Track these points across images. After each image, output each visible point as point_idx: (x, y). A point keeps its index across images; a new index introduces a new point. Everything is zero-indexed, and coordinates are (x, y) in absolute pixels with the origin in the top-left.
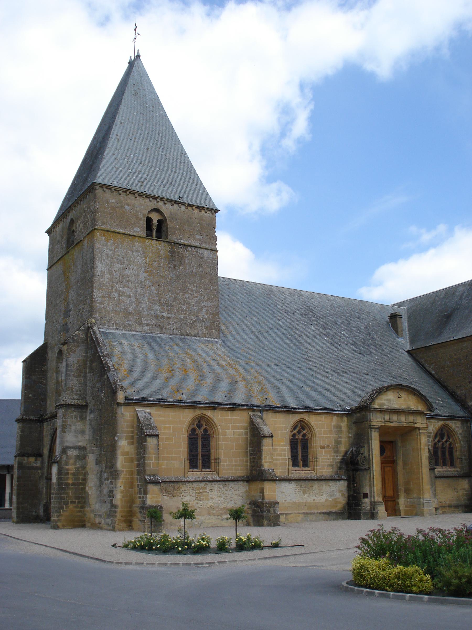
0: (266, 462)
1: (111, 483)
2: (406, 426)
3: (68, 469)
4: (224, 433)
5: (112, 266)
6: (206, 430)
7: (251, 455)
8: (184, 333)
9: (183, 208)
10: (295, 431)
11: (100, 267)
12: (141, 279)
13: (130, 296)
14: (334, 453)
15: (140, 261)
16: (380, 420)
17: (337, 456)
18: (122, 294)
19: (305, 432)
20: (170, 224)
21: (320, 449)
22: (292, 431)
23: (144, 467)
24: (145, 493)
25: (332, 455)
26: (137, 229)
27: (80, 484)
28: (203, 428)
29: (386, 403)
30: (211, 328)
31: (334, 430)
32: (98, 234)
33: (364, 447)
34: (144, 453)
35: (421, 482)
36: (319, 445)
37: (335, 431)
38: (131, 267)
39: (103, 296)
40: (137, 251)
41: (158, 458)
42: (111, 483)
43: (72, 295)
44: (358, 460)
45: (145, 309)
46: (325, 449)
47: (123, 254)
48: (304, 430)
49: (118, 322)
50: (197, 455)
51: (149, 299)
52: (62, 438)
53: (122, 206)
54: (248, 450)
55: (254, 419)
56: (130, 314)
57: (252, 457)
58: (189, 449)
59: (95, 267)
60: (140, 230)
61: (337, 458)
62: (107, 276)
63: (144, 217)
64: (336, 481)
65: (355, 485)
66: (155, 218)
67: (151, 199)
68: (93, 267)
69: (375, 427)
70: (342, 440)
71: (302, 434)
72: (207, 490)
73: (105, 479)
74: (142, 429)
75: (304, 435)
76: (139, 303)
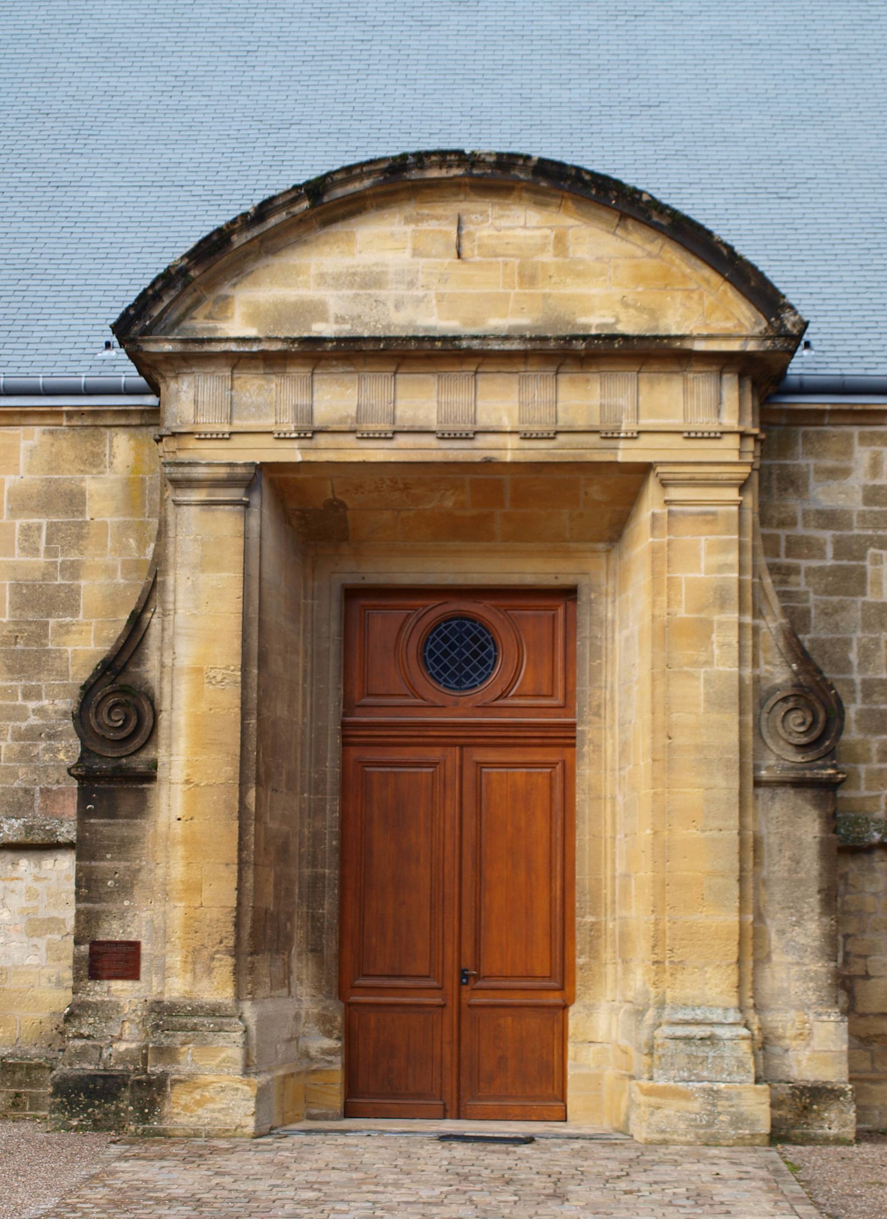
2: (521, 457)
14: (10, 670)
16: (268, 423)
31: (19, 522)
37: (27, 531)
61: (32, 705)
69: (201, 472)
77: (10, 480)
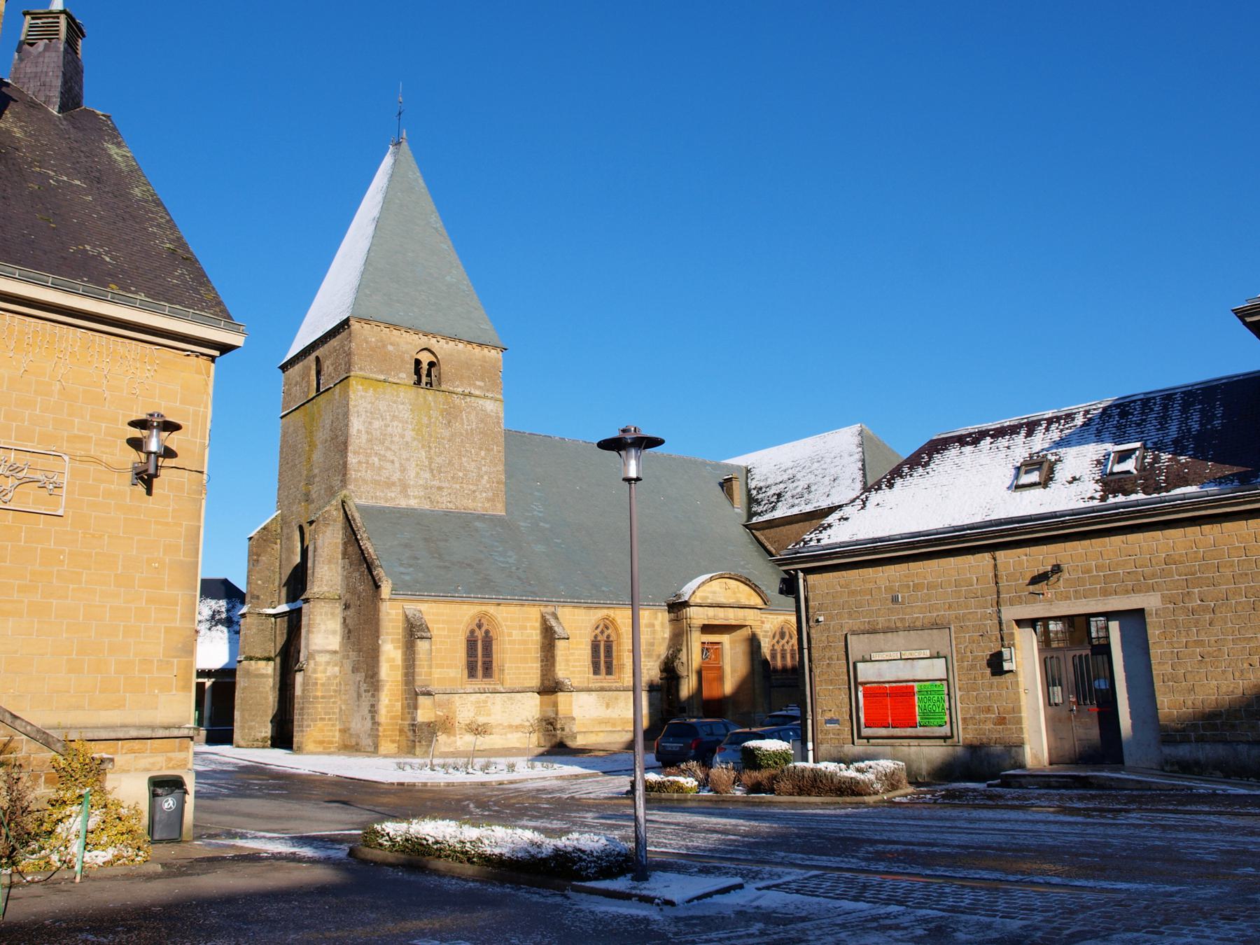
0: (560, 670)
1: (373, 696)
3: (316, 679)
4: (510, 635)
5: (370, 423)
6: (487, 632)
7: (542, 661)
8: (460, 506)
9: (461, 345)
11: (356, 425)
12: (408, 439)
13: (393, 462)
15: (406, 416)
18: (382, 458)
20: (444, 368)
23: (413, 677)
24: (416, 707)
26: (403, 375)
27: (331, 697)
28: (483, 629)
29: (710, 596)
30: (493, 500)
32: (353, 381)
34: (414, 661)
38: (395, 423)
39: (360, 462)
40: (403, 404)
41: (430, 667)
42: (373, 696)
43: (317, 456)
45: (412, 477)
47: (385, 408)
49: (378, 494)
50: (477, 662)
51: (417, 465)
52: (307, 639)
53: (384, 346)
55: (548, 617)
56: (393, 484)
58: (468, 654)
59: (350, 424)
60: (407, 376)
62: (364, 437)
63: (411, 359)
66: (425, 358)
67: (421, 335)
68: (347, 425)
72: (489, 704)
73: (365, 691)
74: (411, 631)
75: (608, 637)
76: (404, 470)
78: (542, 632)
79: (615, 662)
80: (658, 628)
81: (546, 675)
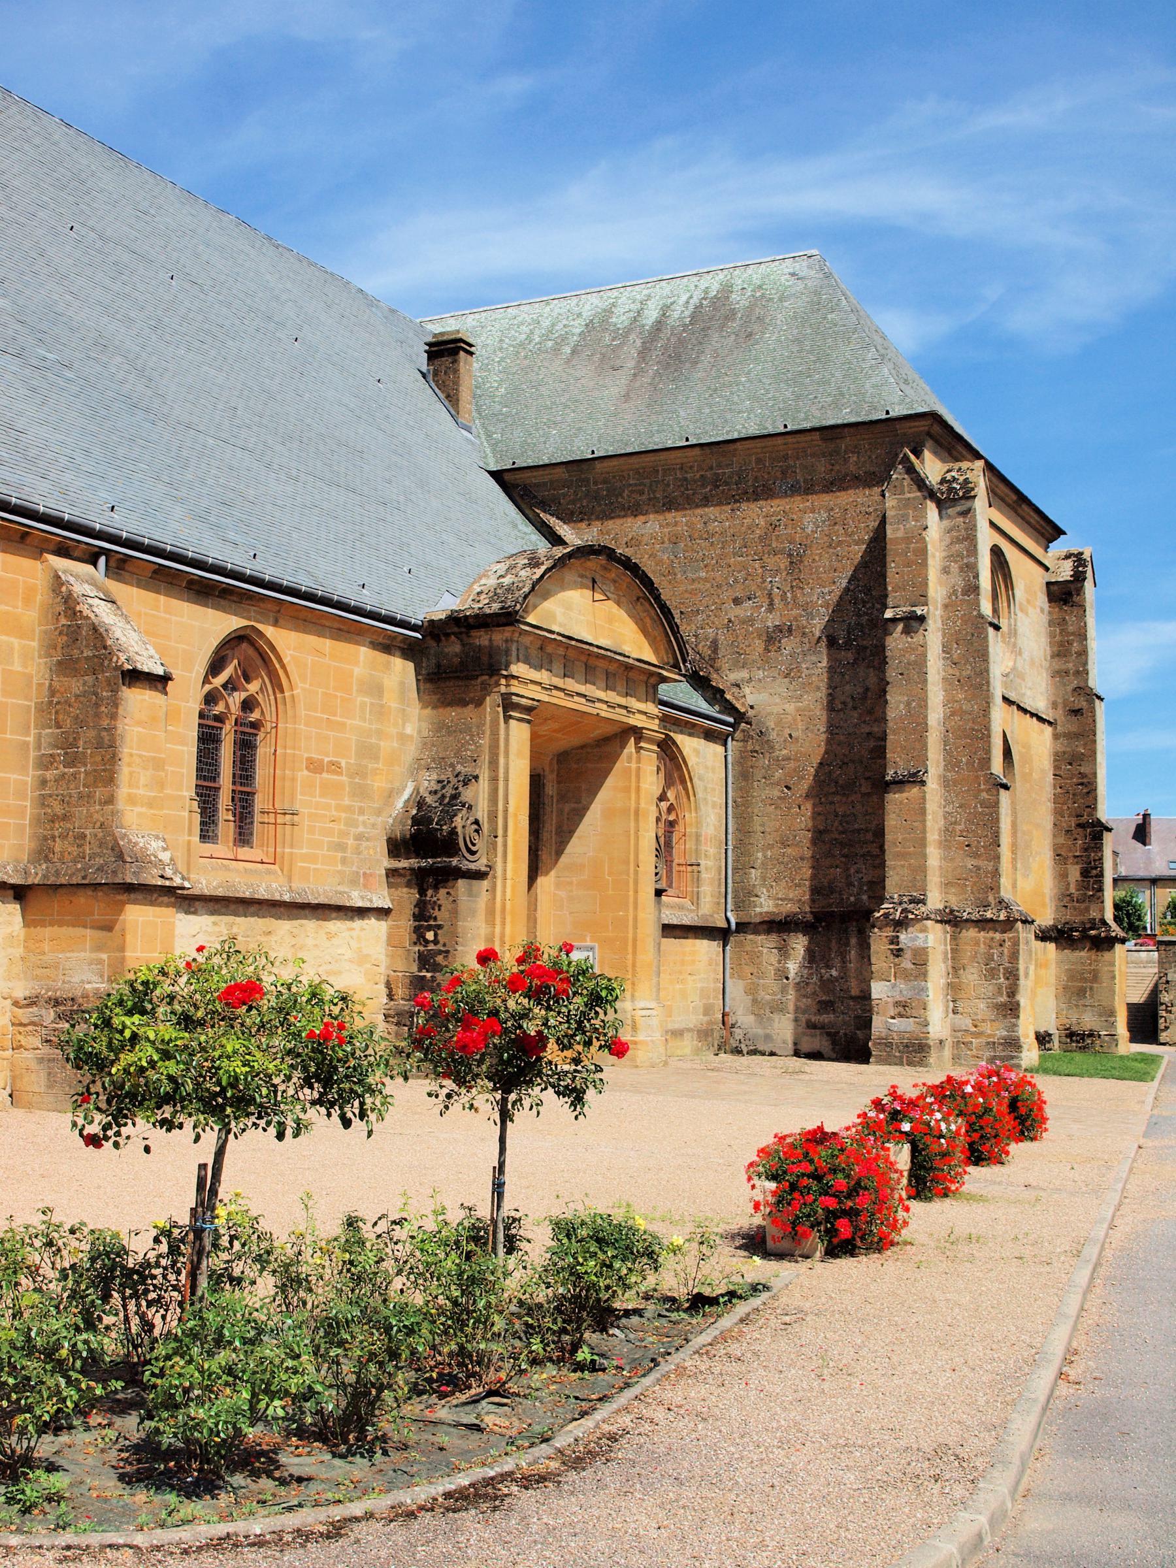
0: (132, 800)
7: (45, 763)
10: (219, 681)
17: (362, 811)
19: (253, 687)
21: (306, 772)
22: (206, 681)
25: (347, 802)
33: (476, 778)
35: (630, 936)
36: (306, 755)
37: (363, 704)
44: (453, 832)
46: (325, 775)
48: (248, 680)
54: (31, 739)
55: (79, 589)
57: (49, 775)
61: (361, 818)
64: (350, 914)
65: (430, 936)
70: (382, 743)
71: (244, 695)
77: (357, 671)
78: (49, 647)
79: (259, 803)
80: (391, 701)
81: (65, 818)
